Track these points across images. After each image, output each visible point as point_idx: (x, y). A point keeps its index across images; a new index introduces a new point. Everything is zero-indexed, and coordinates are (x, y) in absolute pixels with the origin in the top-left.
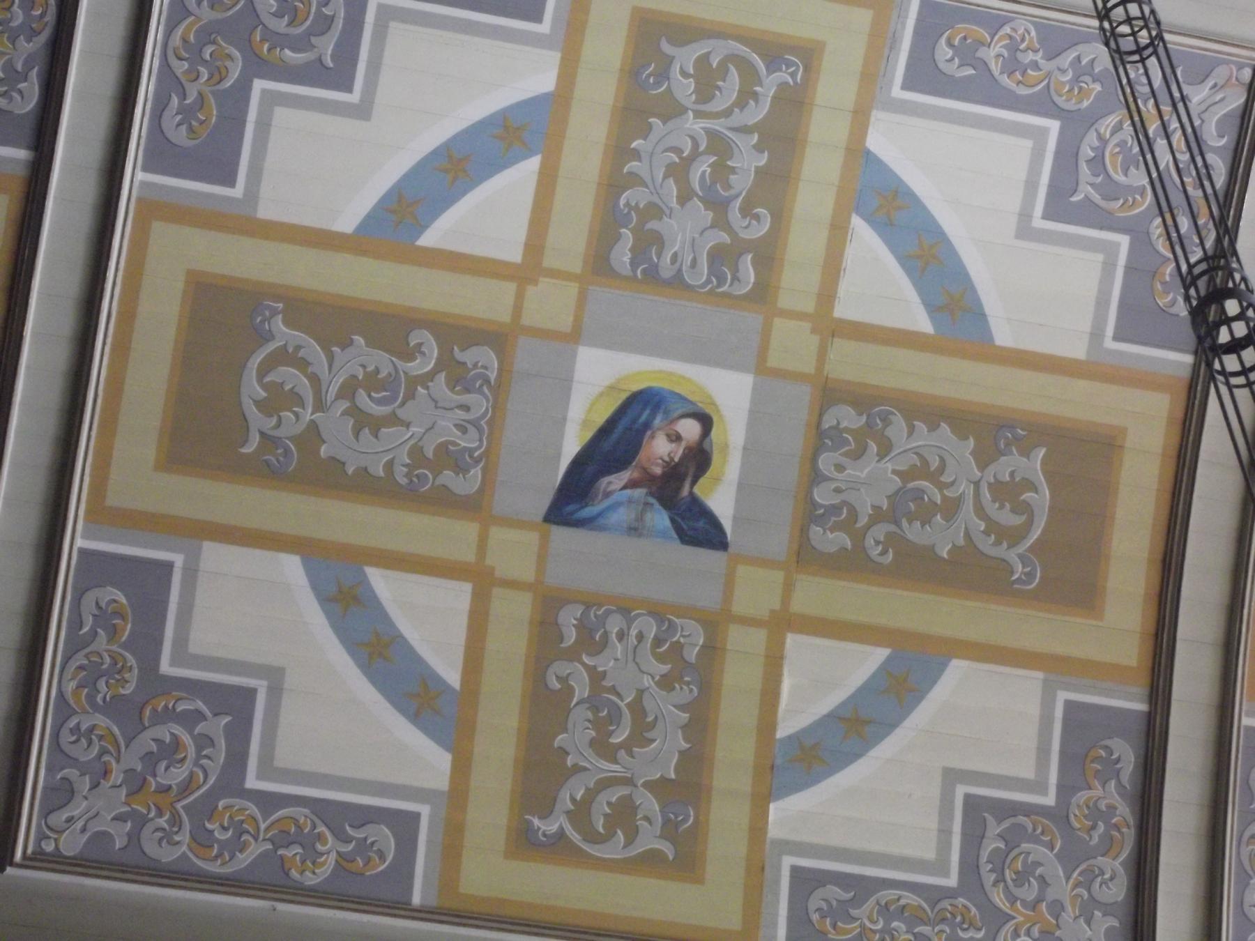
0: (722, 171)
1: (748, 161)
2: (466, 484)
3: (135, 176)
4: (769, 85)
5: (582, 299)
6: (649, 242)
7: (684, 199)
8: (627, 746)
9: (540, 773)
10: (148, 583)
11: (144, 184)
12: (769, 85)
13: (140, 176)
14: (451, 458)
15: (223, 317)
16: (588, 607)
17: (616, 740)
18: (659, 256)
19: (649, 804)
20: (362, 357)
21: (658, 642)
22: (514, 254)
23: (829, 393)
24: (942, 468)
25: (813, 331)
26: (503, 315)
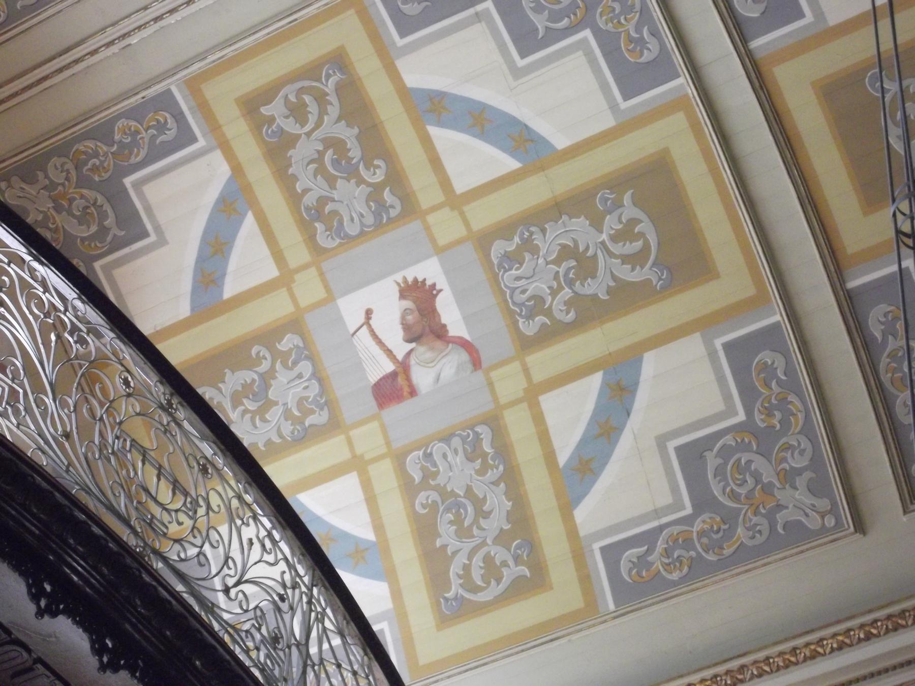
0: (458, 521)
1: (447, 534)
2: (498, 248)
3: (778, 317)
4: (455, 589)
5: (495, 399)
6: (473, 452)
7: (469, 490)
8: (321, 154)
9: (357, 108)
10: (632, 78)
11: (775, 314)
12: (455, 589)
13: (777, 318)
14: (512, 259)
15: (685, 262)
16: (389, 219)
17: (330, 153)
18: (464, 449)
19: (290, 126)
20: (596, 287)
21: (341, 223)
22: (543, 399)
23: (334, 426)
24: (253, 420)
25: (362, 456)
26: (531, 359)
